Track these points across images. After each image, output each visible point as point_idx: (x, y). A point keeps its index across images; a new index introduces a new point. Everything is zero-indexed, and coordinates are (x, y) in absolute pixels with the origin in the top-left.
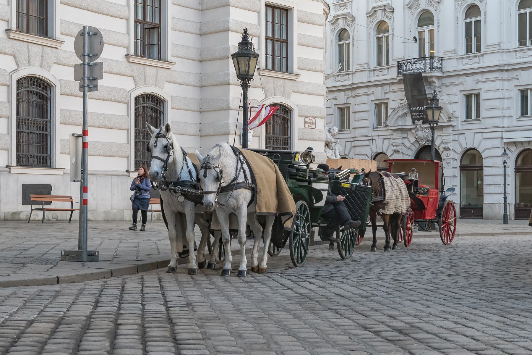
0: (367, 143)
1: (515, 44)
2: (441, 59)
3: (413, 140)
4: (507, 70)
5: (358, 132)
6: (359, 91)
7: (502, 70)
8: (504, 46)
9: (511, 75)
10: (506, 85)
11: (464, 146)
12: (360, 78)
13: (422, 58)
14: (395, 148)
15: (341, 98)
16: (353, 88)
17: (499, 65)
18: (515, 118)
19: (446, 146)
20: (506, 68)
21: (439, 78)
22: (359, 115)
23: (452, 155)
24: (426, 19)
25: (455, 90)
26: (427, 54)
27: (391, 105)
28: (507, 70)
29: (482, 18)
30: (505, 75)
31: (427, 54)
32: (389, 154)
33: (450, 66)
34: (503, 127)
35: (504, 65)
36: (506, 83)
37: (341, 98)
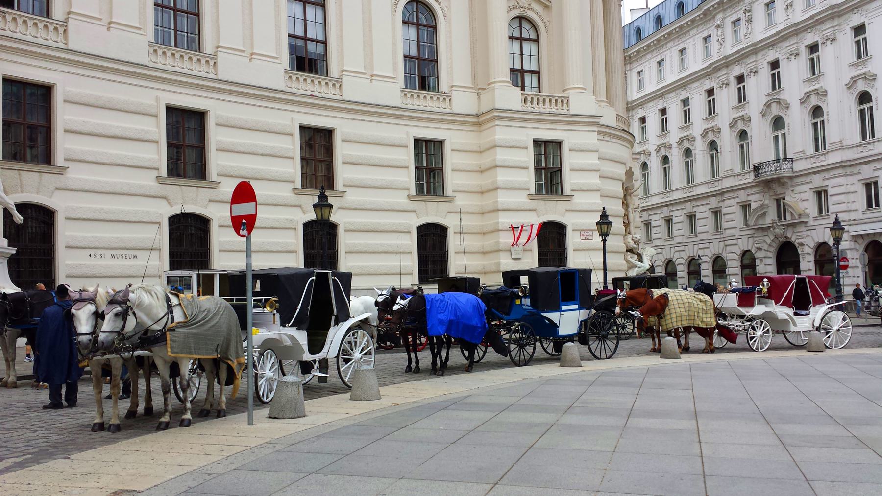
0: (735, 242)
1: (858, 139)
2: (792, 160)
3: (772, 238)
4: (850, 166)
5: (728, 232)
6: (726, 195)
7: (845, 166)
8: (847, 143)
9: (855, 170)
10: (850, 180)
11: (817, 241)
12: (727, 183)
13: (778, 160)
14: (757, 246)
15: (714, 202)
16: (721, 193)
17: (841, 162)
18: (861, 210)
19: (800, 241)
20: (848, 163)
21: (791, 178)
22: (727, 217)
23: (807, 250)
24: (778, 123)
25: (805, 188)
26: (781, 156)
27: (754, 206)
28: (850, 166)
29: (825, 118)
30: (848, 170)
31: (781, 156)
32: (753, 251)
33: (799, 166)
34: (849, 221)
35: (850, 161)
36: (849, 178)
37: (714, 202)
